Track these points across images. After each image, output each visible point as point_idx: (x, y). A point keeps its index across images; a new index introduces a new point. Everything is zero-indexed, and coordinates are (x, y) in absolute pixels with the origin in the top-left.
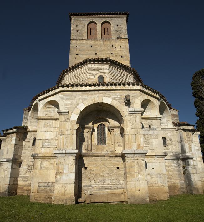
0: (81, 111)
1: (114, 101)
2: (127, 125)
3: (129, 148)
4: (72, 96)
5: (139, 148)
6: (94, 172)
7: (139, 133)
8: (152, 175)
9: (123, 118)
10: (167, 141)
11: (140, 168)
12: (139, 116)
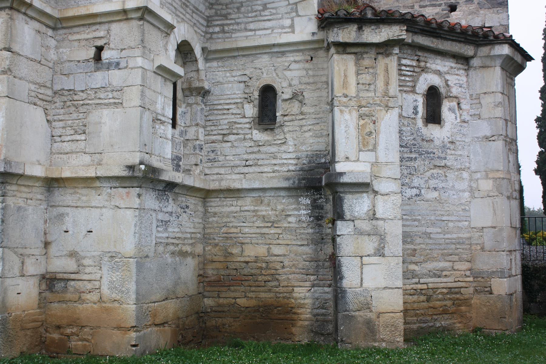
8: (84, 258)
10: (279, 102)
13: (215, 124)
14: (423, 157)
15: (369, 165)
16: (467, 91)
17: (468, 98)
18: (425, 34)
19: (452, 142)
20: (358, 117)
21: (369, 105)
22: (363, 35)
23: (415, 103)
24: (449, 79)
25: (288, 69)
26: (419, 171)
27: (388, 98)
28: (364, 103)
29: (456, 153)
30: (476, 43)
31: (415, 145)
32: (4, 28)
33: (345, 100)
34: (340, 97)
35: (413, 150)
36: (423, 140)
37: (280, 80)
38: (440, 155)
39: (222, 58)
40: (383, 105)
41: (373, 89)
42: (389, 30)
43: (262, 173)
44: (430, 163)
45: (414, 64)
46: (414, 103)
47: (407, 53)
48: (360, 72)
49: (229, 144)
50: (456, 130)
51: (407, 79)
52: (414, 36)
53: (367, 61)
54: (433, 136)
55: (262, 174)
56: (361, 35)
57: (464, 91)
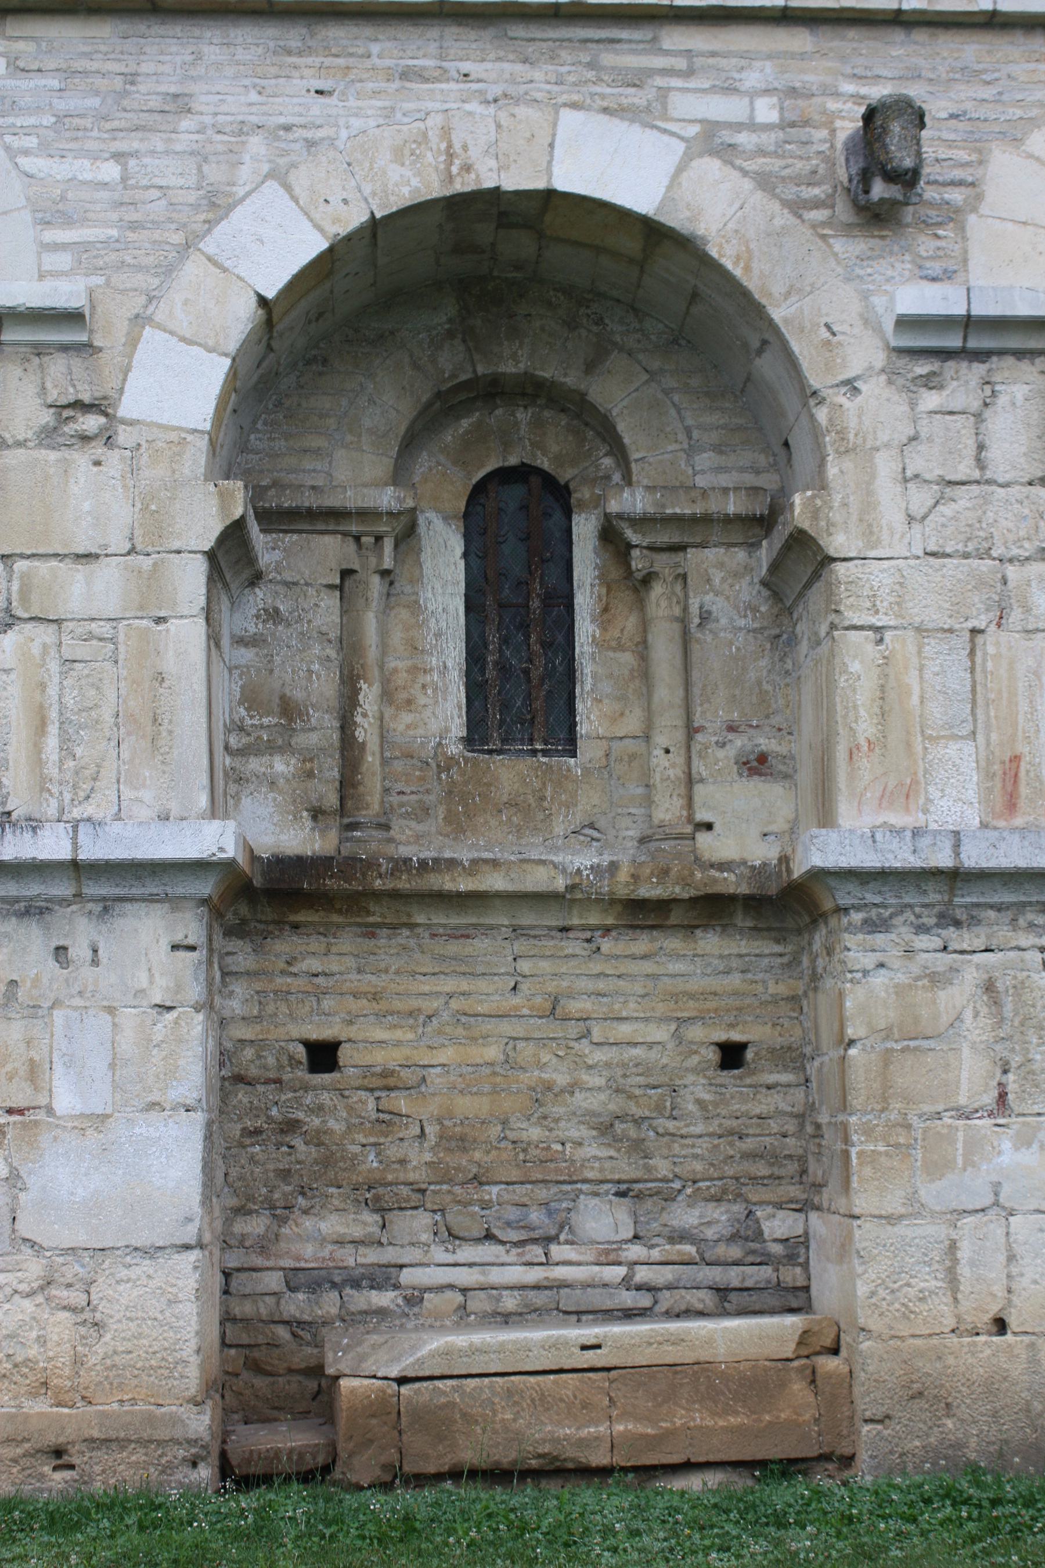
0: (263, 301)
1: (711, 167)
2: (869, 504)
3: (886, 799)
4: (132, 78)
5: (1011, 805)
6: (432, 1108)
7: (1015, 616)
9: (822, 415)
11: (1016, 1060)
12: (1020, 391)
32: (1036, 415)
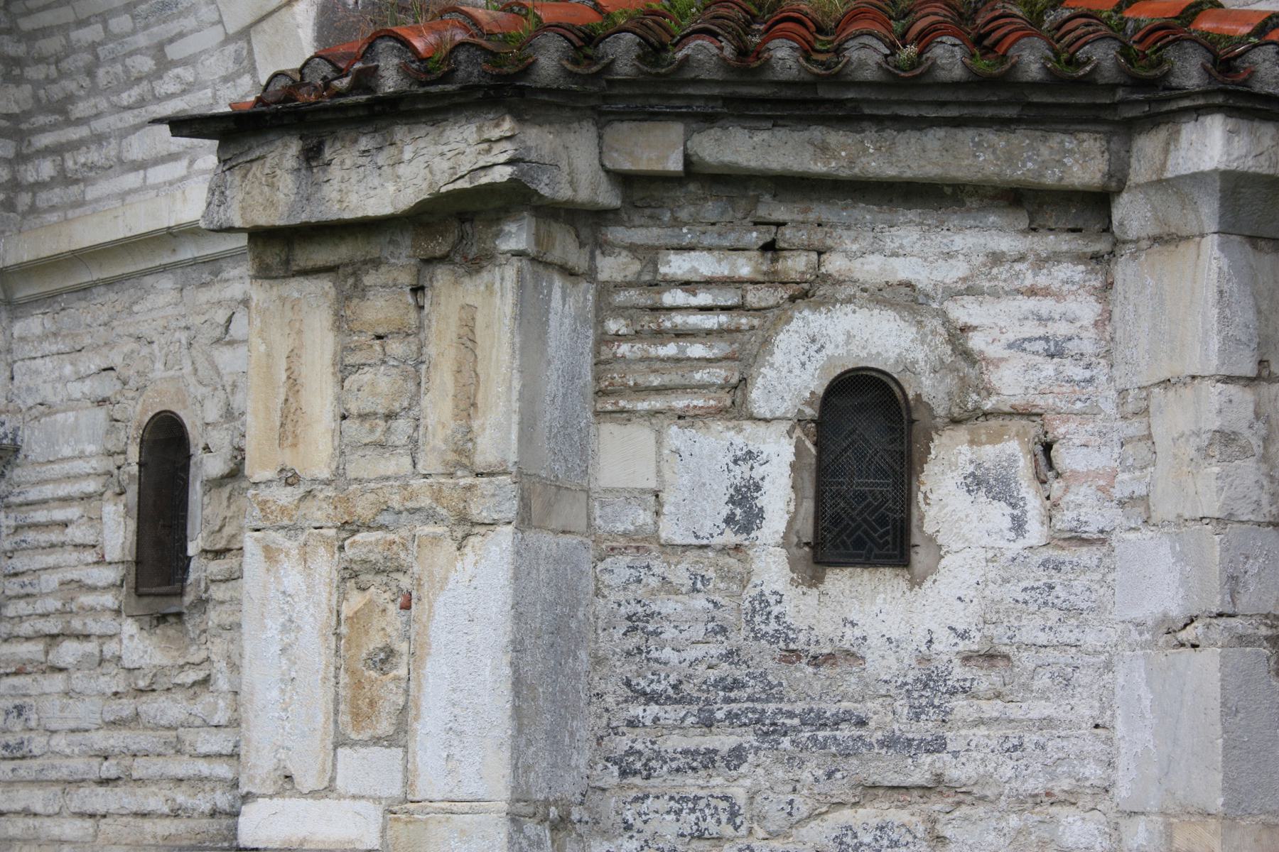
10: (196, 492)
13: (29, 590)
14: (786, 742)
15: (374, 813)
16: (1101, 371)
17: (1109, 408)
18: (768, 118)
19: (991, 657)
20: (336, 577)
21: (385, 518)
22: (326, 188)
23: (741, 471)
24: (973, 322)
25: (225, 338)
26: (761, 818)
27: (469, 480)
28: (363, 509)
29: (1014, 711)
30: (1103, 115)
31: (737, 684)
33: (285, 496)
34: (268, 483)
35: (720, 715)
36: (791, 656)
37: (202, 390)
38: (903, 726)
39: (52, 297)
40: (444, 512)
41: (404, 440)
42: (432, 149)
43: (144, 815)
44: (830, 775)
45: (744, 267)
46: (737, 470)
47: (694, 221)
48: (350, 360)
49: (58, 682)
50: (1014, 590)
51: (697, 350)
52: (696, 138)
53: (380, 303)
54: (858, 632)
55: (139, 821)
56: (317, 184)
57: (1079, 373)
